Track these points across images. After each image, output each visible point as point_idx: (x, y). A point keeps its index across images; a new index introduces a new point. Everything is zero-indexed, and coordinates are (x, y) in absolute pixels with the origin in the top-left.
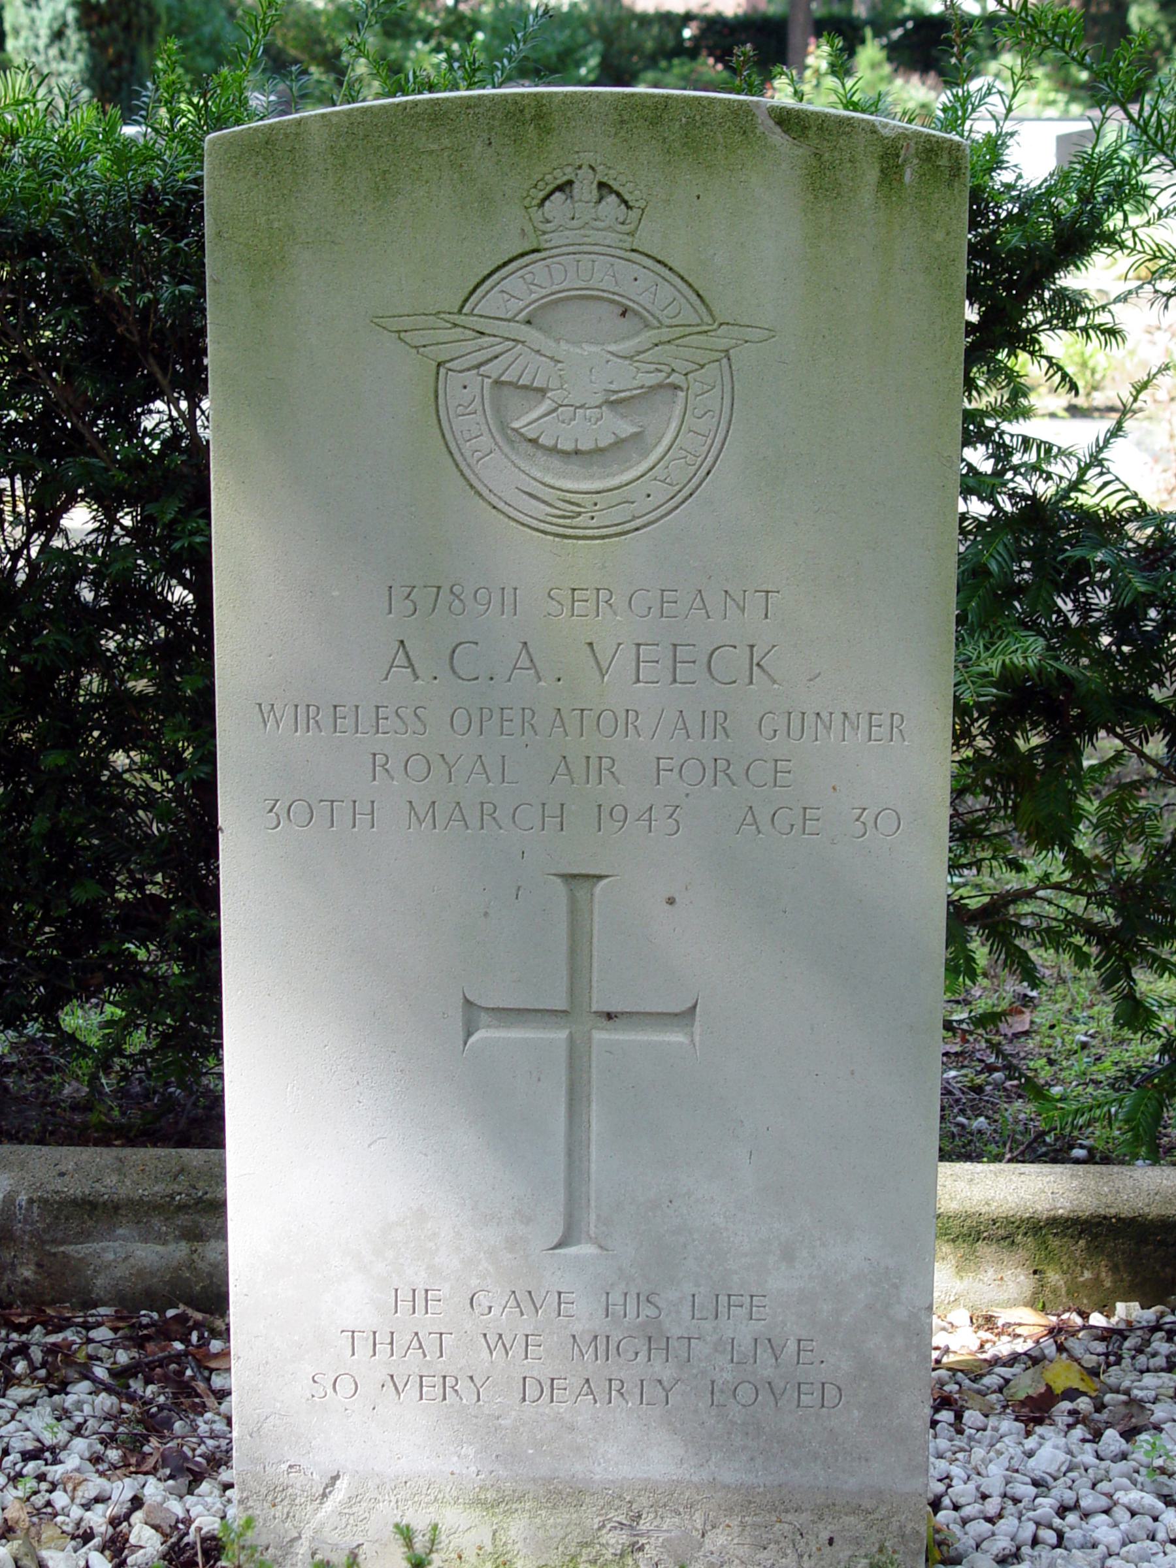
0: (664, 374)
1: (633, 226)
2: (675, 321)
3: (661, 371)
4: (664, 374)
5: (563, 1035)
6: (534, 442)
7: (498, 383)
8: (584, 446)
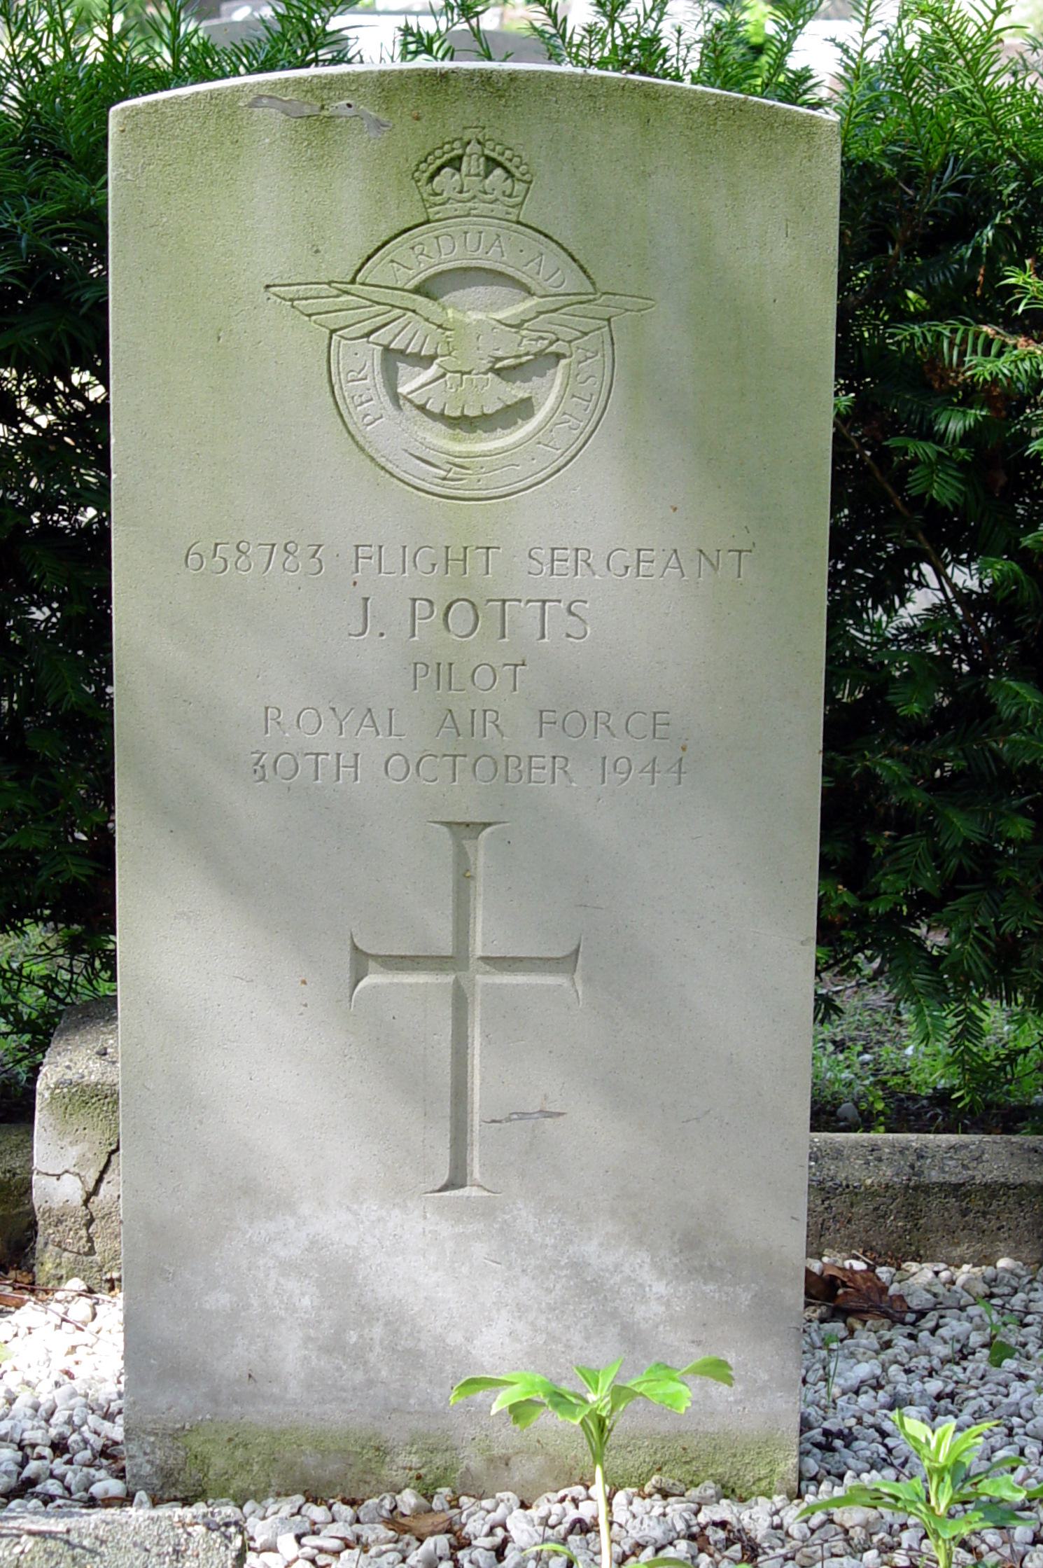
0: (546, 342)
1: (519, 199)
3: (542, 338)
4: (546, 342)
5: (450, 979)
6: (422, 408)
7: (387, 349)
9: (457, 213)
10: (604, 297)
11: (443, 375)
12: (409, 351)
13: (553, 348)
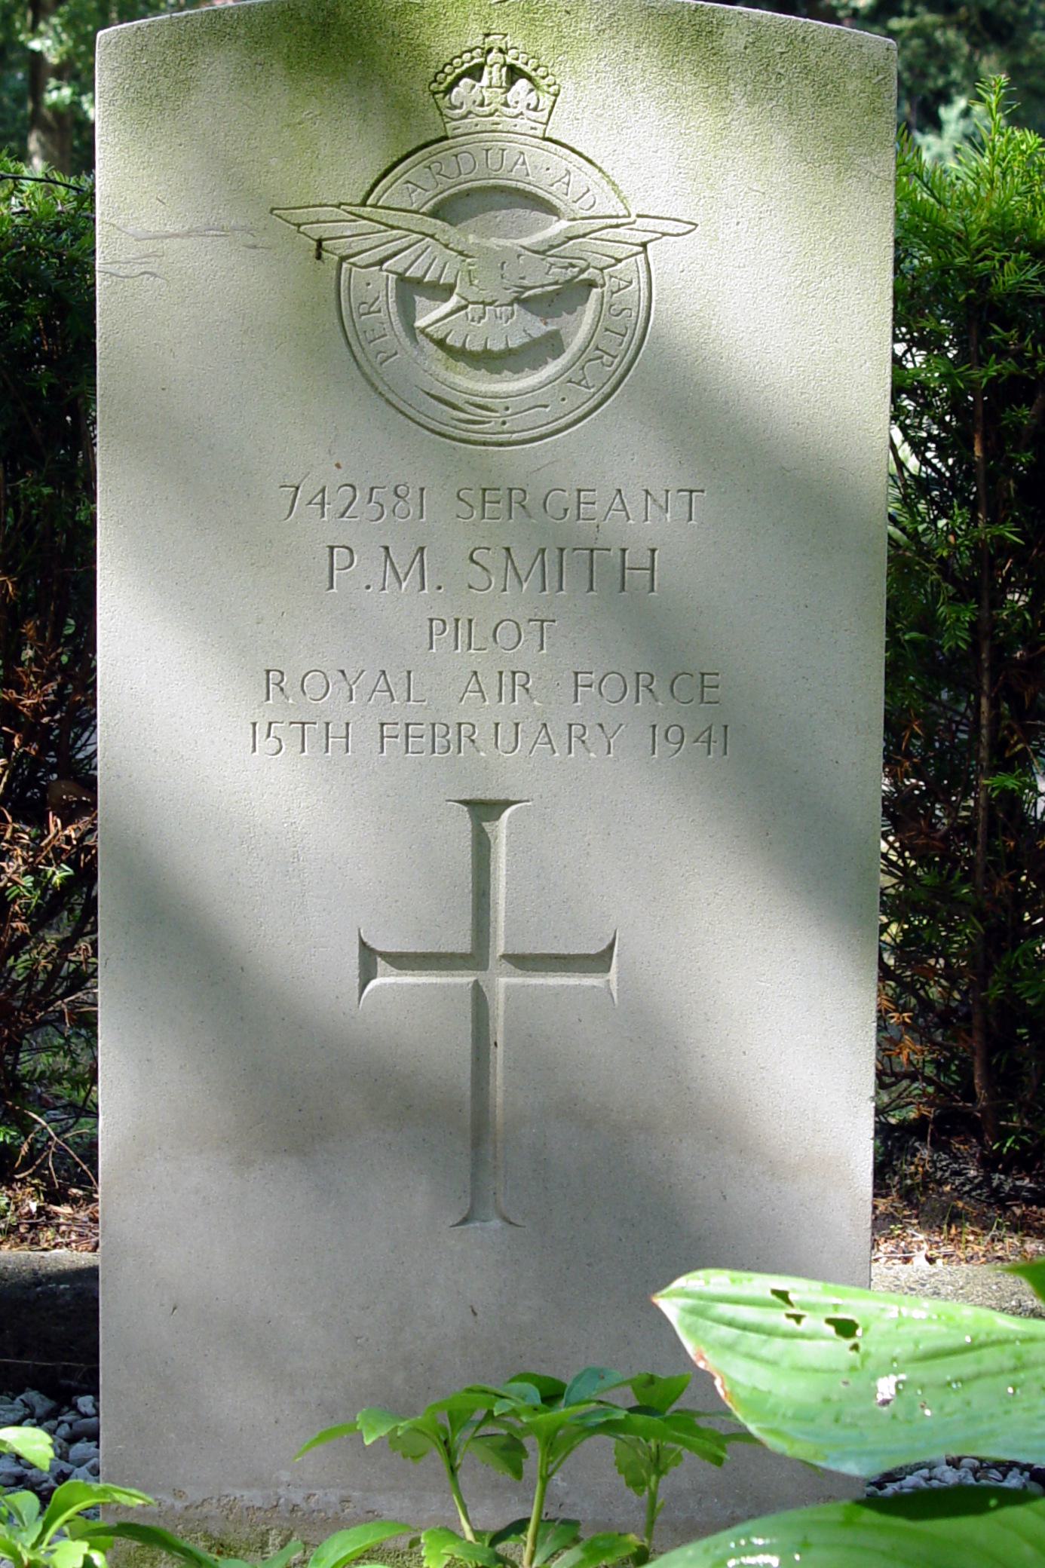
2: (590, 213)
3: (573, 266)
5: (464, 979)
7: (402, 279)
8: (496, 346)
9: (478, 128)
10: (639, 220)
11: (466, 307)
12: (426, 279)
13: (585, 276)
